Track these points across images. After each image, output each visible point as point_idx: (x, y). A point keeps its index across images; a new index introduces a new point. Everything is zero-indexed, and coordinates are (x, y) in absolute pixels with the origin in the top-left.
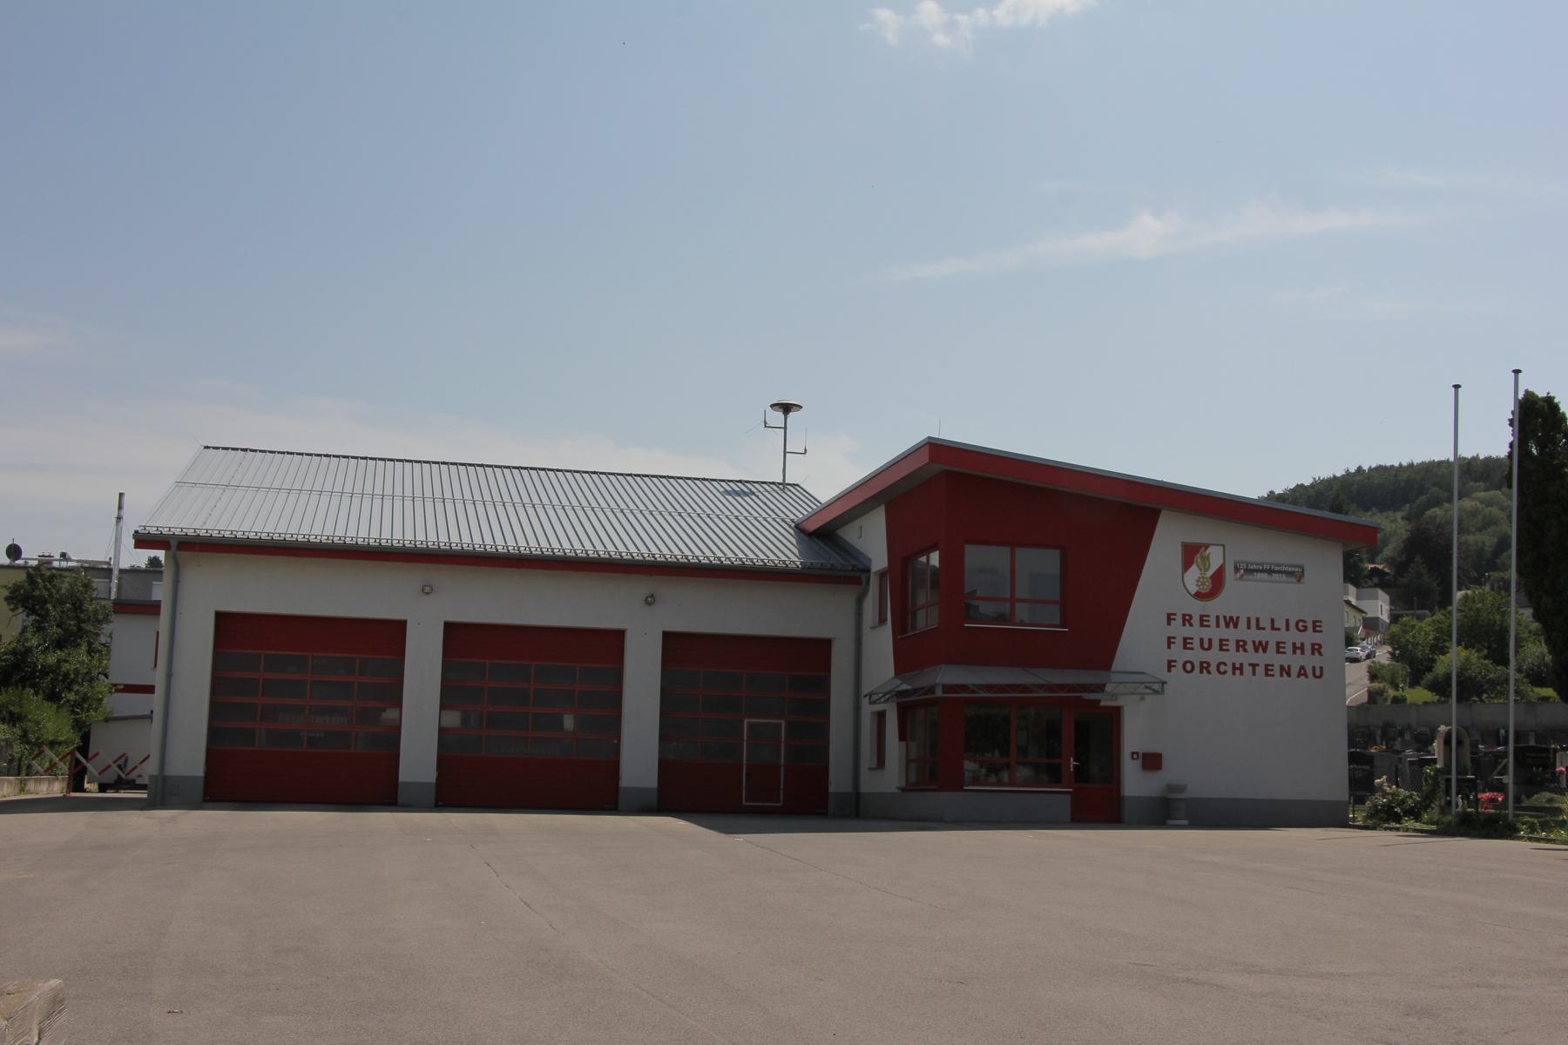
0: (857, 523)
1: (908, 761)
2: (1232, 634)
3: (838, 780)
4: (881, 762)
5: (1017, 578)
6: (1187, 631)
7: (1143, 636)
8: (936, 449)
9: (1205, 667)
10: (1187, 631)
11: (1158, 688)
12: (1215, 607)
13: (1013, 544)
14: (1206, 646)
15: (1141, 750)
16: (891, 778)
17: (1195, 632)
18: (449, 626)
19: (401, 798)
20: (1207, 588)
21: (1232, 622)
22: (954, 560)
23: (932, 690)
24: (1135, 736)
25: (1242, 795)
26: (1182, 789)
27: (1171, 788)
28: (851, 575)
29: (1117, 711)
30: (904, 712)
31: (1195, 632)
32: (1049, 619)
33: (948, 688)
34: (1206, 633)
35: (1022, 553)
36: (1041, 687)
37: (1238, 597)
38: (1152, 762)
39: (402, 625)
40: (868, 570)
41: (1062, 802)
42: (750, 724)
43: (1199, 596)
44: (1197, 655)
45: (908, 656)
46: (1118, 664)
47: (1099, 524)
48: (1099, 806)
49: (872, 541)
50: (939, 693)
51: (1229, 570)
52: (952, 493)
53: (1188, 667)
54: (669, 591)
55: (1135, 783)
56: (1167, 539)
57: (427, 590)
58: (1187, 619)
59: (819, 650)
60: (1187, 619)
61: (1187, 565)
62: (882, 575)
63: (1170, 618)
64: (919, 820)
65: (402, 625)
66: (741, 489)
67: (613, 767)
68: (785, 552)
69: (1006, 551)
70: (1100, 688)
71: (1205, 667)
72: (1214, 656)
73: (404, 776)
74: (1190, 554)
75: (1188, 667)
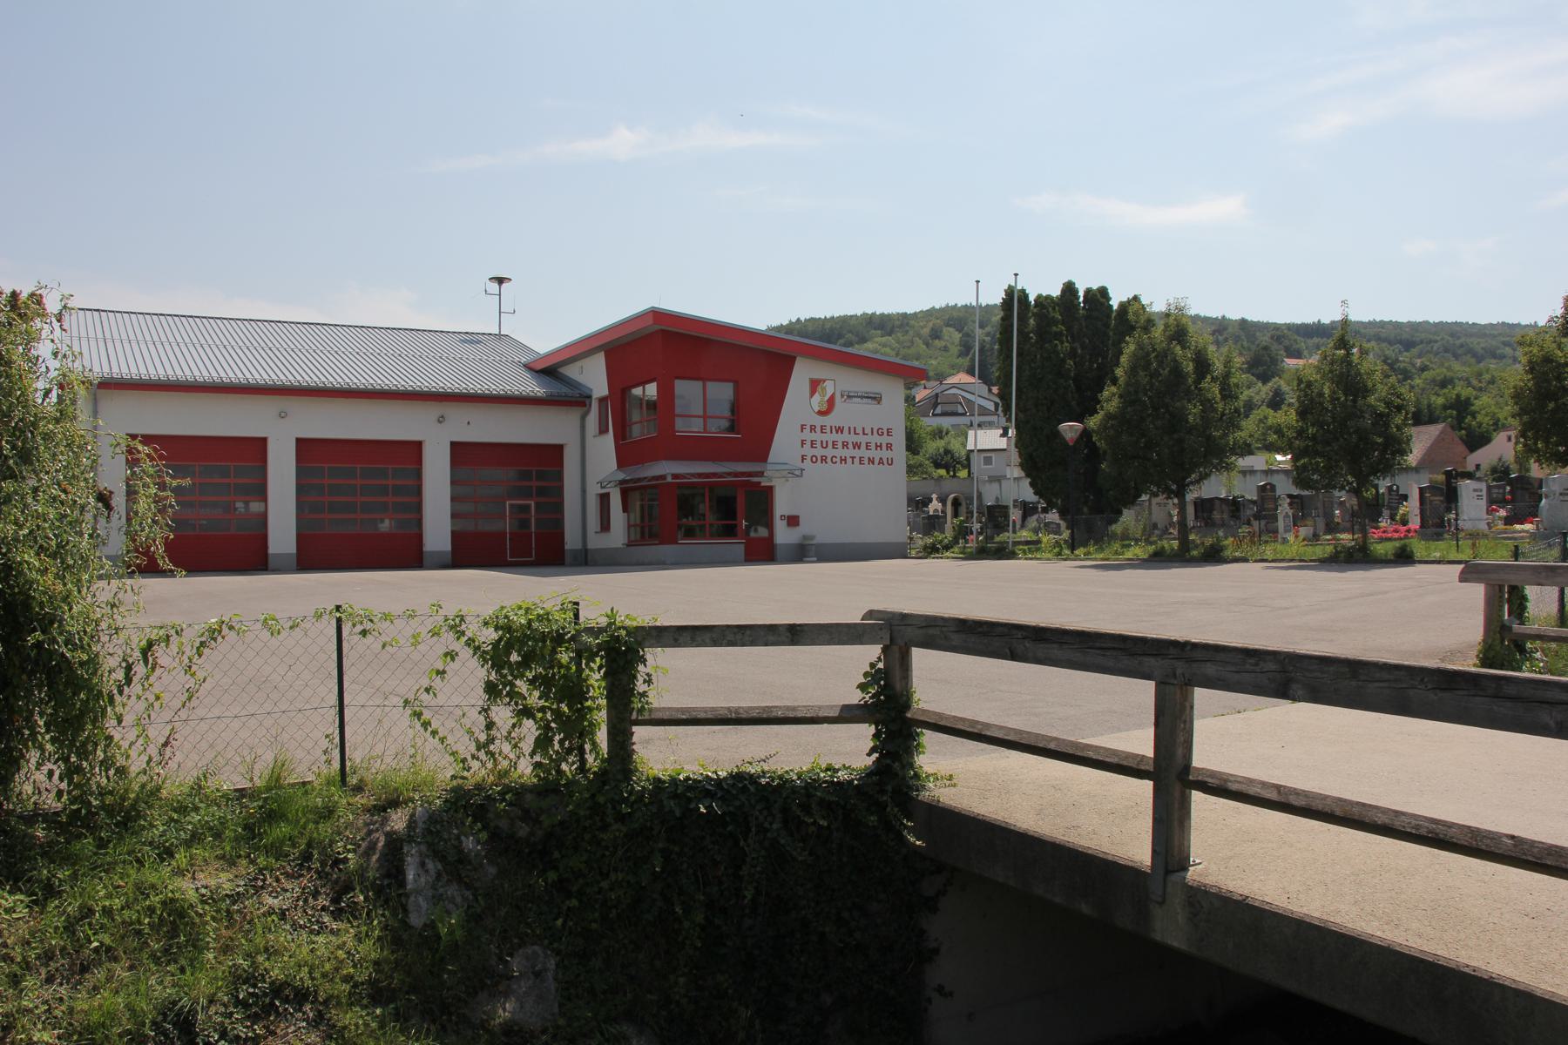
0: (578, 364)
1: (629, 526)
2: (840, 438)
3: (571, 540)
4: (605, 526)
5: (702, 403)
6: (813, 436)
7: (786, 442)
8: (657, 315)
9: (824, 459)
10: (813, 436)
11: (797, 473)
12: (828, 421)
13: (703, 379)
14: (824, 446)
15: (787, 514)
16: (618, 535)
17: (818, 436)
18: (453, 444)
19: (426, 560)
20: (824, 408)
21: (840, 430)
22: (666, 392)
23: (663, 477)
24: (781, 506)
25: (868, 540)
26: (812, 538)
27: (805, 537)
28: (578, 400)
29: (770, 489)
30: (625, 494)
31: (818, 436)
32: (717, 428)
33: (675, 476)
34: (825, 437)
35: (710, 385)
36: (729, 474)
37: (844, 413)
38: (793, 521)
39: (264, 440)
40: (590, 397)
41: (739, 549)
42: (512, 506)
43: (820, 413)
44: (819, 452)
45: (626, 455)
46: (771, 459)
47: (756, 365)
48: (763, 552)
49: (594, 377)
50: (669, 479)
51: (838, 396)
52: (661, 348)
53: (814, 459)
54: (455, 412)
55: (784, 536)
56: (802, 373)
57: (282, 415)
58: (813, 428)
59: (553, 454)
60: (813, 428)
61: (813, 392)
62: (602, 400)
63: (803, 428)
64: (643, 564)
65: (264, 440)
66: (471, 339)
67: (419, 538)
68: (531, 386)
69: (700, 384)
70: (761, 474)
71: (824, 459)
72: (829, 452)
73: (271, 551)
74: (815, 385)
75: (814, 459)
